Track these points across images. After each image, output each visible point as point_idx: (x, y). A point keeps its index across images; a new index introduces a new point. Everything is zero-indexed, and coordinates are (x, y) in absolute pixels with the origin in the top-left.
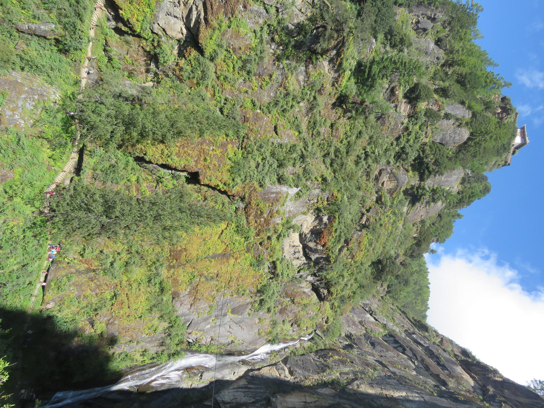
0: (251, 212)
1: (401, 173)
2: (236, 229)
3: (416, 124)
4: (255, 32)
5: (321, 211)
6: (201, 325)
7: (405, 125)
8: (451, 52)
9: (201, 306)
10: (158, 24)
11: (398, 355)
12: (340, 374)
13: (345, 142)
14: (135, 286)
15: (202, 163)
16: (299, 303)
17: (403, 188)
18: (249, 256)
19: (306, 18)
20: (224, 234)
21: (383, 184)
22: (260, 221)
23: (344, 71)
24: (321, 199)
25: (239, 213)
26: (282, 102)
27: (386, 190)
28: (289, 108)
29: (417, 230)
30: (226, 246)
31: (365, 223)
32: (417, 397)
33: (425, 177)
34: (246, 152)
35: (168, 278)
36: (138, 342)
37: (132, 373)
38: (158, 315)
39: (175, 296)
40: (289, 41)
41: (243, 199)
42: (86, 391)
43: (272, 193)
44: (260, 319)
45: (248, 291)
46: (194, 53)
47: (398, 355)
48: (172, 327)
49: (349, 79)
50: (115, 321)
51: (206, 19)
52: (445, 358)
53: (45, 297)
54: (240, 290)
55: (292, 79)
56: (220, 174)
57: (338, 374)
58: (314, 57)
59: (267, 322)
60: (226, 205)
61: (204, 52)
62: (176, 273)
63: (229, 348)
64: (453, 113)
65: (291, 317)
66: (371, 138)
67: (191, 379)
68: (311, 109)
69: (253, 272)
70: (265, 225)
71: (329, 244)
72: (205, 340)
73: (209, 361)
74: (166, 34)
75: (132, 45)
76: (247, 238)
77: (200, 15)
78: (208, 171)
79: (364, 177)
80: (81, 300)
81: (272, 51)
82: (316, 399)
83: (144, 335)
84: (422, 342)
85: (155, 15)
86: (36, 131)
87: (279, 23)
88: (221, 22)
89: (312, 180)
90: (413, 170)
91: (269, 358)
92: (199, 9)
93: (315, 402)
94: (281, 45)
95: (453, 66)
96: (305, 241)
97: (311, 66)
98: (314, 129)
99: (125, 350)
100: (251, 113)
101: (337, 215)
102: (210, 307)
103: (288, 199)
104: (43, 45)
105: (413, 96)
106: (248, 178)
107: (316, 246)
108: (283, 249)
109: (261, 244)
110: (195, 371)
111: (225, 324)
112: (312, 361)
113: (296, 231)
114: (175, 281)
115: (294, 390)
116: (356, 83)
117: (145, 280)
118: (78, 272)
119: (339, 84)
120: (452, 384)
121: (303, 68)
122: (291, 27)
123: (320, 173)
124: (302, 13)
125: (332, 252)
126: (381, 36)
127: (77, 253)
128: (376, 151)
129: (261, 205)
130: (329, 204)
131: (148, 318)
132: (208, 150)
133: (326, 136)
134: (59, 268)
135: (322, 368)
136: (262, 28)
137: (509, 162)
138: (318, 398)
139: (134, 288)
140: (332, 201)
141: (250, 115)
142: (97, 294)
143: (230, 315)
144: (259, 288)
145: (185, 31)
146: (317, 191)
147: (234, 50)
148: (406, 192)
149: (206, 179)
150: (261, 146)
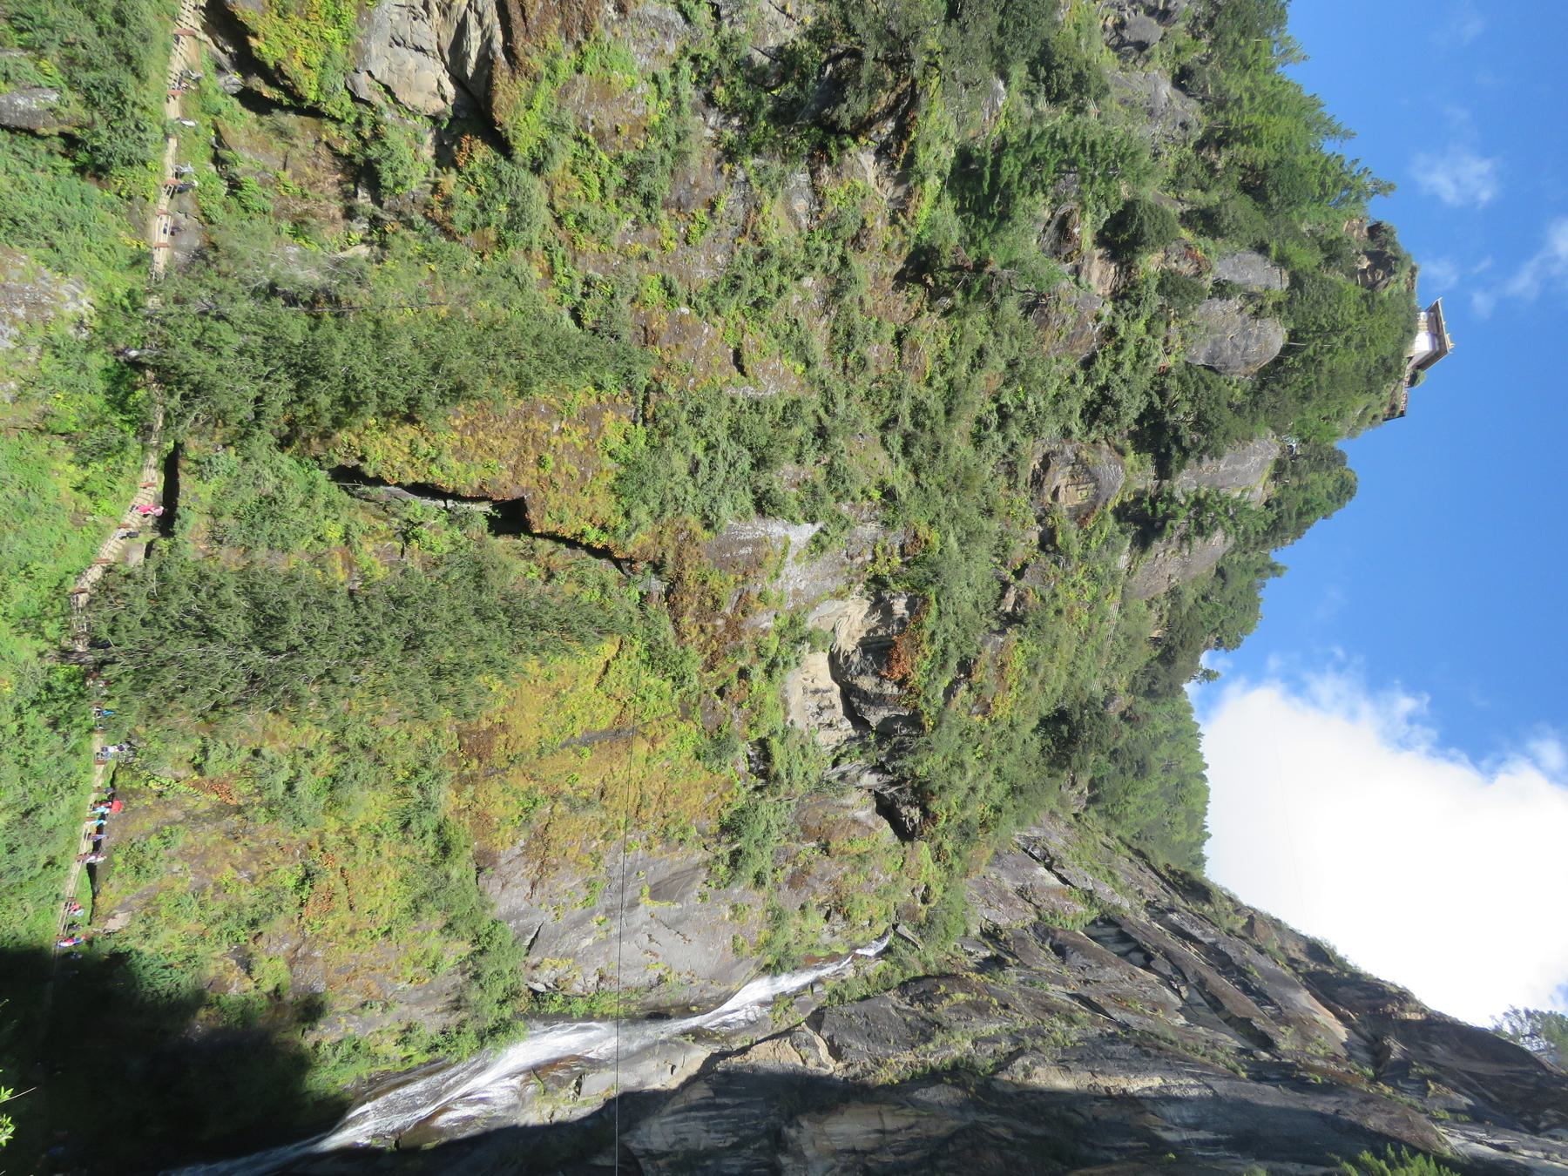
0: (685, 604)
1: (1104, 462)
2: (645, 656)
3: (1137, 316)
4: (655, 79)
5: (885, 585)
6: (567, 938)
7: (1105, 321)
8: (1221, 106)
9: (563, 886)
10: (370, 73)
11: (1133, 976)
12: (975, 1043)
13: (939, 381)
14: (364, 843)
15: (533, 471)
16: (843, 853)
17: (1114, 503)
18: (691, 733)
19: (799, 30)
20: (611, 672)
21: (1055, 495)
22: (715, 627)
23: (923, 180)
24: (884, 549)
25: (651, 608)
26: (751, 279)
27: (1066, 513)
28: (773, 296)
29: (1161, 617)
30: (619, 708)
31: (1014, 609)
32: (1193, 1086)
33: (1173, 466)
34: (657, 432)
35: (459, 812)
36: (386, 1006)
37: (377, 1096)
38: (438, 921)
39: (484, 862)
40: (759, 102)
41: (658, 568)
42: (243, 1160)
43: (743, 544)
44: (734, 908)
45: (693, 832)
46: (483, 152)
47: (1133, 976)
48: (482, 952)
49: (938, 199)
50: (312, 949)
51: (509, 52)
52: (1262, 971)
53: (99, 900)
54: (672, 829)
55: (773, 210)
56: (587, 499)
57: (968, 1044)
58: (832, 144)
59: (756, 914)
60: (613, 587)
61: (511, 148)
62: (481, 797)
63: (652, 998)
64: (1237, 279)
65: (823, 894)
66: (1012, 365)
67: (548, 1096)
68: (836, 294)
69: (705, 776)
70: (729, 637)
71: (916, 678)
72: (583, 981)
73: (599, 1040)
74: (396, 101)
75: (295, 141)
76: (679, 680)
77: (490, 40)
78: (550, 493)
79: (1002, 480)
80: (208, 897)
81: (709, 133)
82: (912, 1120)
83: (401, 985)
84: (1196, 933)
85: (357, 48)
86: (27, 414)
87: (723, 50)
88: (556, 55)
89: (853, 499)
90: (1139, 448)
91: (770, 1016)
92: (487, 21)
93: (910, 1127)
94: (735, 114)
95: (1227, 146)
96: (845, 673)
97: (825, 169)
98: (848, 351)
99: (351, 1031)
100: (664, 318)
101: (931, 592)
102: (589, 884)
103: (789, 558)
104: (27, 154)
105: (1122, 237)
106: (670, 507)
107: (879, 685)
108: (785, 701)
109: (721, 692)
110: (560, 1073)
111: (636, 931)
112: (893, 1012)
113: (820, 647)
114: (482, 821)
115: (847, 1101)
116: (958, 211)
117: (393, 824)
118: (193, 818)
119: (910, 216)
120: (1286, 1042)
121: (803, 178)
122: (761, 59)
123: (875, 476)
124: (789, 16)
125: (927, 701)
126: (1019, 72)
127: (184, 763)
128: (1030, 400)
129: (714, 582)
130: (907, 564)
131: (410, 934)
132: (547, 432)
133: (883, 368)
134: (135, 810)
135: (923, 1032)
136: (676, 68)
137: (1401, 406)
138: (918, 1116)
139: (361, 850)
140: (915, 554)
141: (660, 322)
142: (253, 878)
143: (647, 904)
144: (726, 818)
145: (450, 90)
146: (871, 529)
147: (600, 136)
148: (1121, 513)
149: (547, 518)
150: (698, 412)
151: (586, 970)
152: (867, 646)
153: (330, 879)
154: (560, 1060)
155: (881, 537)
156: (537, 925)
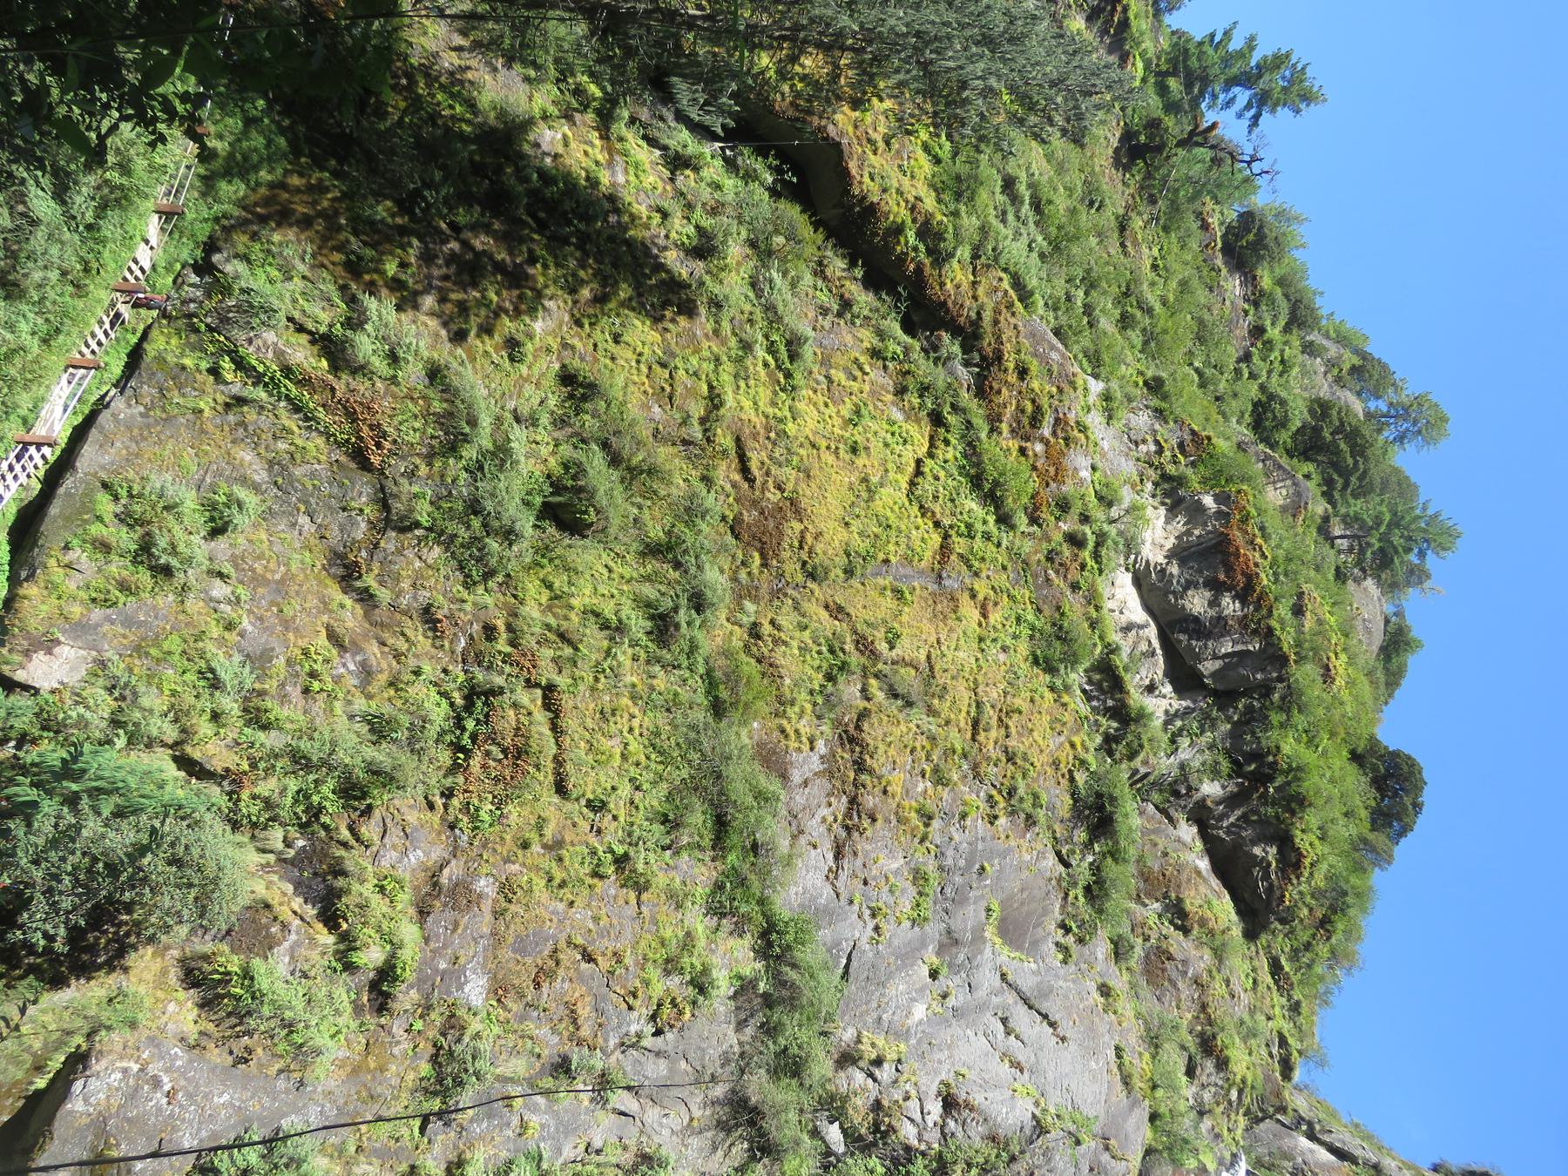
6: (891, 991)
14: (593, 640)
44: (1105, 990)
50: (475, 875)
62: (767, 629)
69: (1049, 695)
76: (1004, 520)
102: (919, 877)
107: (1214, 603)
111: (981, 1008)
142: (367, 672)
151: (923, 1080)
155: (1157, 427)
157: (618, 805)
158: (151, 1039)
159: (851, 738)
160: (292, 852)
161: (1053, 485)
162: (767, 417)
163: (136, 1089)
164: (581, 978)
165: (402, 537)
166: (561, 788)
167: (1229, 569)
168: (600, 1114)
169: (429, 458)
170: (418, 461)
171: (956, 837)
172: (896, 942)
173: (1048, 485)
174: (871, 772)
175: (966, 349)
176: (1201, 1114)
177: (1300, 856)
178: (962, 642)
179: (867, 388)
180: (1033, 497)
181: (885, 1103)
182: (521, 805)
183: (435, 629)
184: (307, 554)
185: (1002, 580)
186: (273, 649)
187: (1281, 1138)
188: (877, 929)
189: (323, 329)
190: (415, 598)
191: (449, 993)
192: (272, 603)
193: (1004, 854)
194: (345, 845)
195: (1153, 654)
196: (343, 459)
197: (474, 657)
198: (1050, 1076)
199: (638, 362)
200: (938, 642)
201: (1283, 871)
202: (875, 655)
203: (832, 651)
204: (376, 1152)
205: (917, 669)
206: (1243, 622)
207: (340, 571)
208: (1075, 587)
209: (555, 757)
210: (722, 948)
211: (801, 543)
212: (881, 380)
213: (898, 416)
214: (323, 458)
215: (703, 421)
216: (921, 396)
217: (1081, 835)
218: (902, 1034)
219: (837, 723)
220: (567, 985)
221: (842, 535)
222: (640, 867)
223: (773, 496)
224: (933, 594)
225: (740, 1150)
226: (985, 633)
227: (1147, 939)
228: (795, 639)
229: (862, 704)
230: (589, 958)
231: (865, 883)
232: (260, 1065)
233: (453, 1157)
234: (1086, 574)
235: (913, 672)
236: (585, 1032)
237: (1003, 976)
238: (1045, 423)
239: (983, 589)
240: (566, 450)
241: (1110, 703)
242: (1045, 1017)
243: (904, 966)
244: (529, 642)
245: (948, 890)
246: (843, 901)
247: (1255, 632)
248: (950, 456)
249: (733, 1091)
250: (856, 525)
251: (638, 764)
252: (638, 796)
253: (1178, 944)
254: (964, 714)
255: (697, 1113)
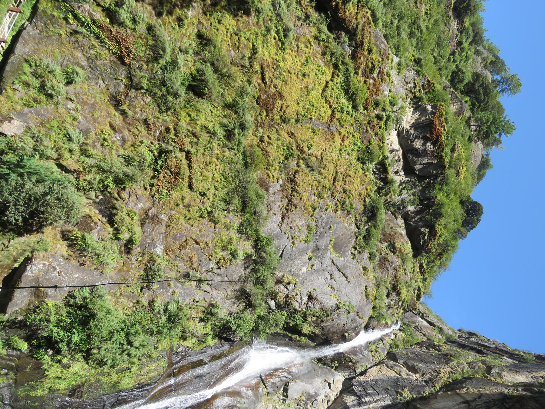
14: (204, 136)
37: (181, 370)
44: (365, 269)
50: (160, 213)
62: (266, 139)
67: (270, 397)
69: (361, 172)
70: (375, 91)
76: (355, 107)
96: (408, 140)
102: (309, 227)
111: (324, 270)
142: (124, 141)
146: (411, 74)
151: (302, 290)
152: (415, 126)
153: (178, 158)
154: (276, 370)
155: (416, 77)
156: (282, 247)
157: (210, 194)
158: (52, 255)
159: (291, 180)
160: (98, 200)
161: (374, 96)
162: (273, 59)
163: (48, 270)
164: (194, 249)
165: (137, 92)
166: (190, 187)
167: (432, 133)
168: (198, 291)
169: (147, 62)
170: (143, 63)
171: (323, 216)
172: (299, 248)
173: (372, 96)
174: (297, 192)
175: (350, 39)
176: (389, 308)
177: (436, 232)
178: (334, 150)
179: (311, 51)
180: (366, 100)
181: (290, 296)
182: (177, 191)
183: (148, 127)
184: (102, 95)
185: (351, 129)
186: (90, 129)
187: (413, 317)
188: (293, 243)
189: (107, 6)
190: (141, 115)
191: (151, 250)
192: (90, 112)
193: (338, 223)
194: (116, 199)
195: (400, 161)
196: (115, 60)
197: (162, 139)
198: (343, 292)
199: (227, 32)
200: (326, 149)
201: (430, 237)
202: (303, 152)
203: (288, 149)
204: (126, 296)
205: (317, 158)
206: (433, 152)
207: (114, 103)
208: (376, 134)
209: (189, 176)
210: (241, 244)
211: (281, 108)
212: (317, 49)
213: (322, 64)
214: (108, 58)
215: (249, 58)
216: (331, 57)
217: (365, 219)
218: (298, 276)
219: (287, 174)
220: (189, 251)
221: (296, 107)
222: (216, 216)
223: (273, 90)
224: (326, 132)
225: (242, 306)
226: (342, 148)
227: (381, 254)
228: (276, 143)
229: (296, 168)
230: (197, 243)
231: (291, 228)
232: (88, 266)
233: (151, 299)
234: (381, 130)
235: (315, 159)
236: (195, 266)
237: (332, 261)
238: (375, 72)
239: (343, 131)
240: (198, 65)
241: (382, 176)
242: (344, 275)
243: (301, 255)
244: (181, 135)
245: (318, 233)
246: (283, 233)
247: (436, 156)
248: (338, 81)
249: (241, 288)
250: (301, 104)
251: (217, 182)
252: (217, 192)
253: (391, 257)
254: (331, 175)
255: (229, 293)
